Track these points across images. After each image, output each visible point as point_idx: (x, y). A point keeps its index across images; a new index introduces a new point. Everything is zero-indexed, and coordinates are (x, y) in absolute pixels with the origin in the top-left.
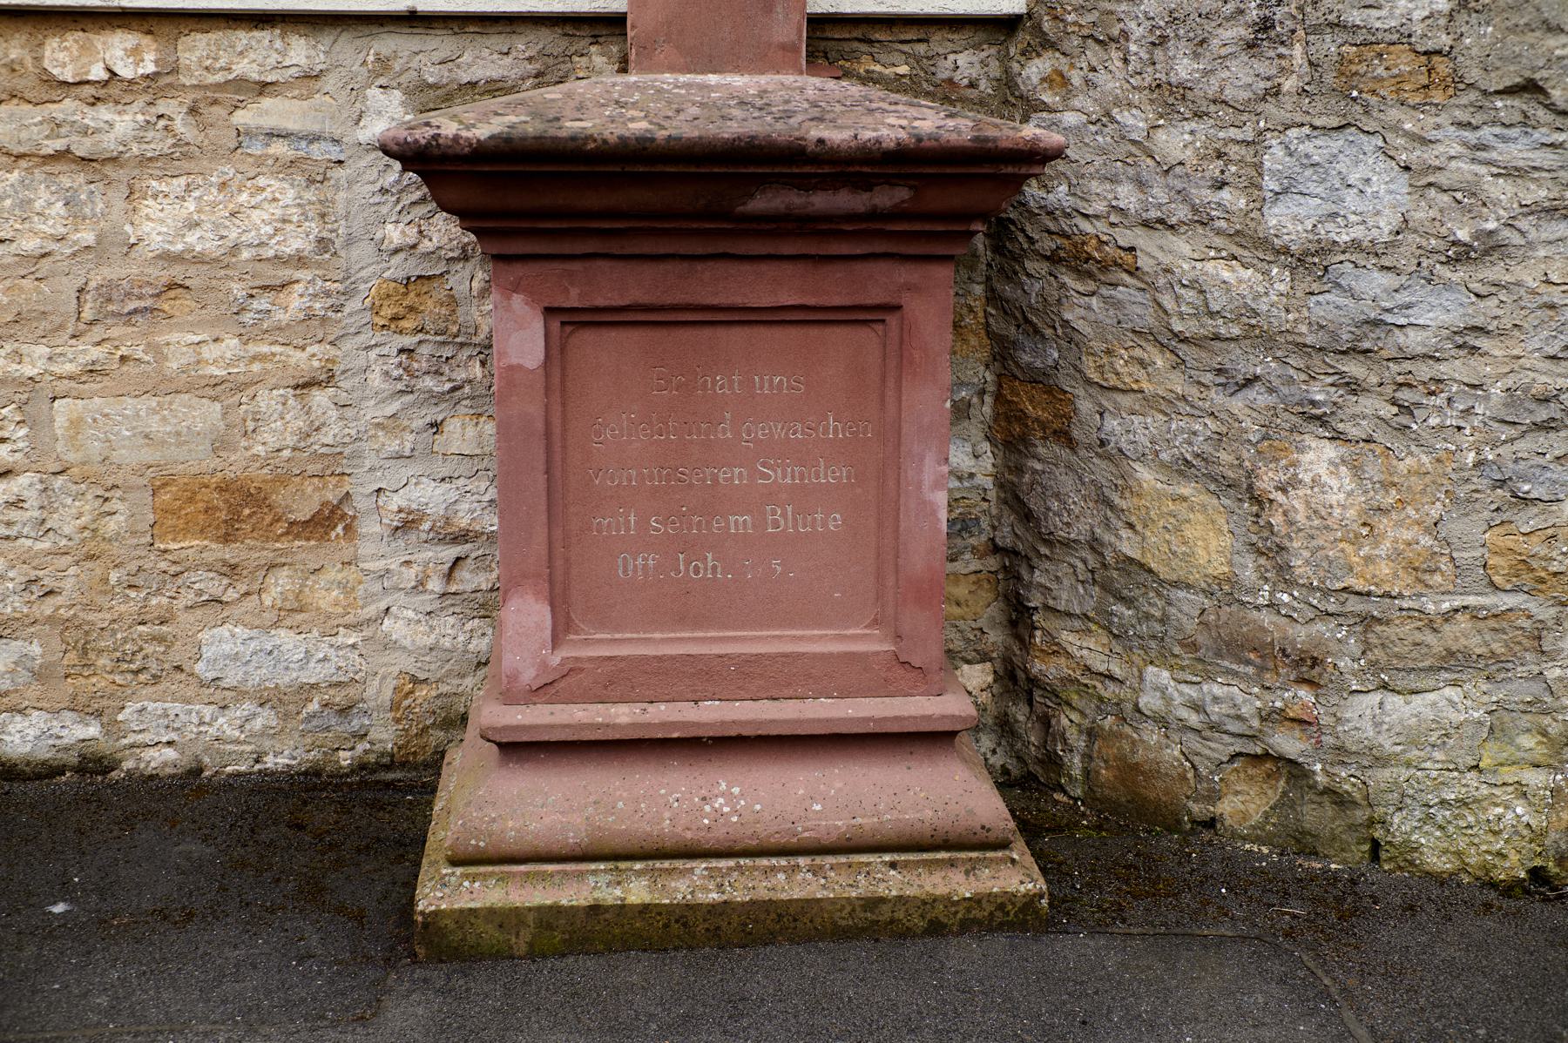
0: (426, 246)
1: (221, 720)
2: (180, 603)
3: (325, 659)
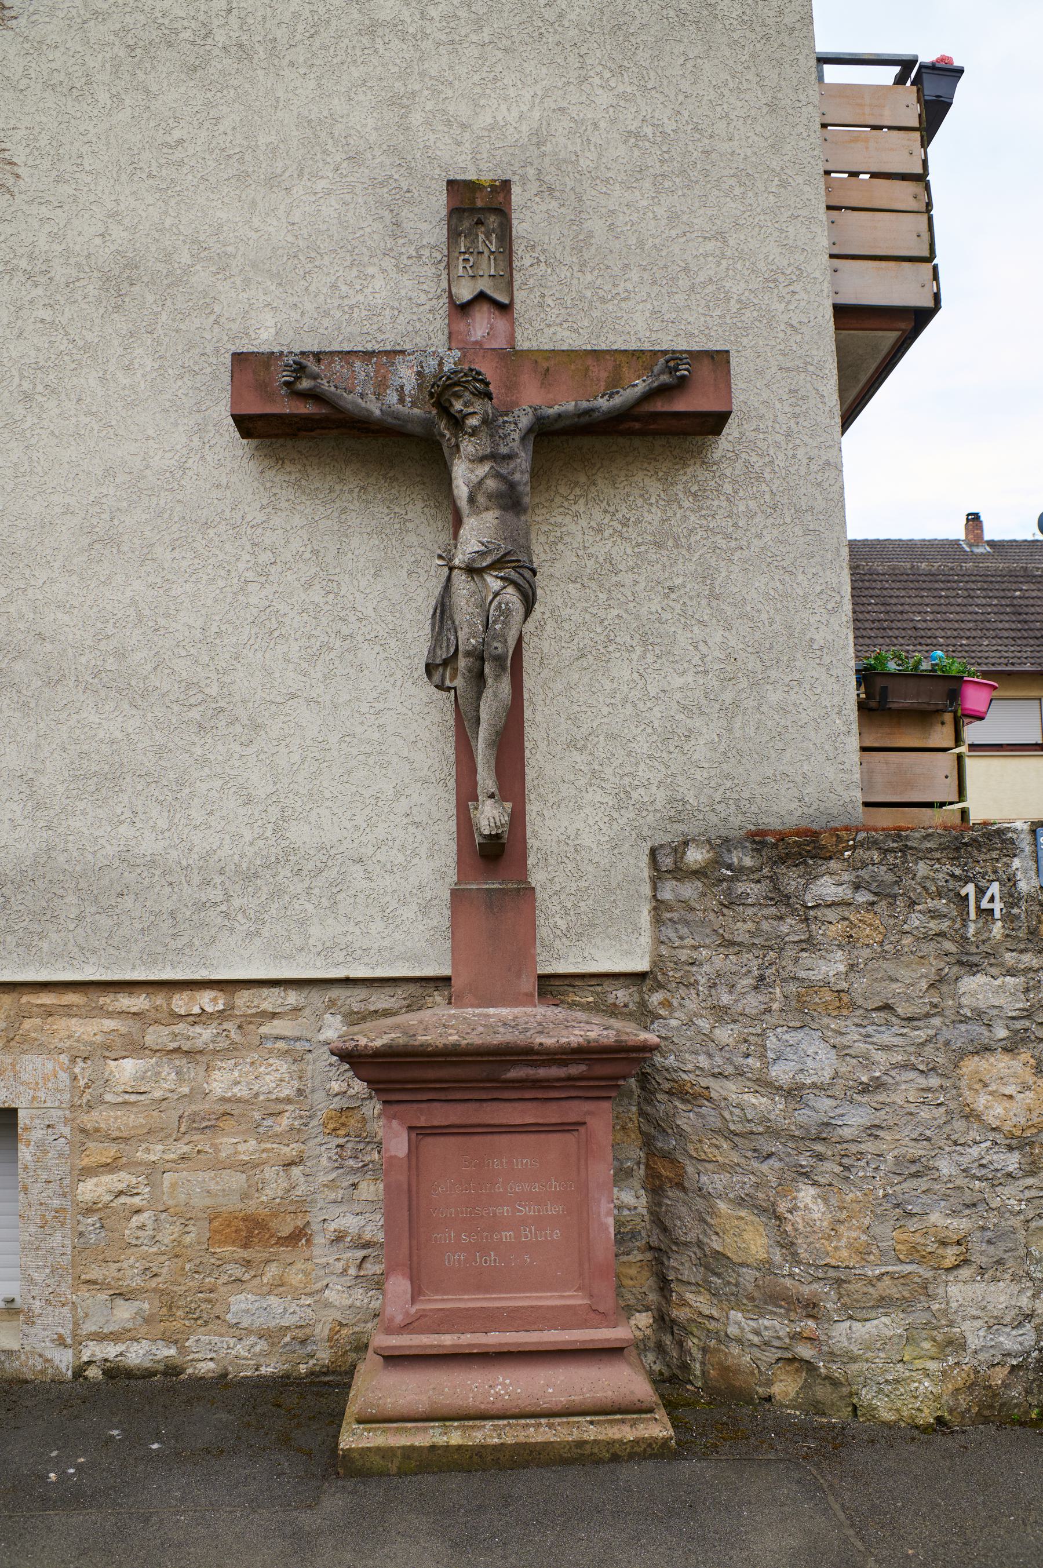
0: (352, 1092)
1: (239, 1346)
2: (220, 1281)
3: (294, 1313)
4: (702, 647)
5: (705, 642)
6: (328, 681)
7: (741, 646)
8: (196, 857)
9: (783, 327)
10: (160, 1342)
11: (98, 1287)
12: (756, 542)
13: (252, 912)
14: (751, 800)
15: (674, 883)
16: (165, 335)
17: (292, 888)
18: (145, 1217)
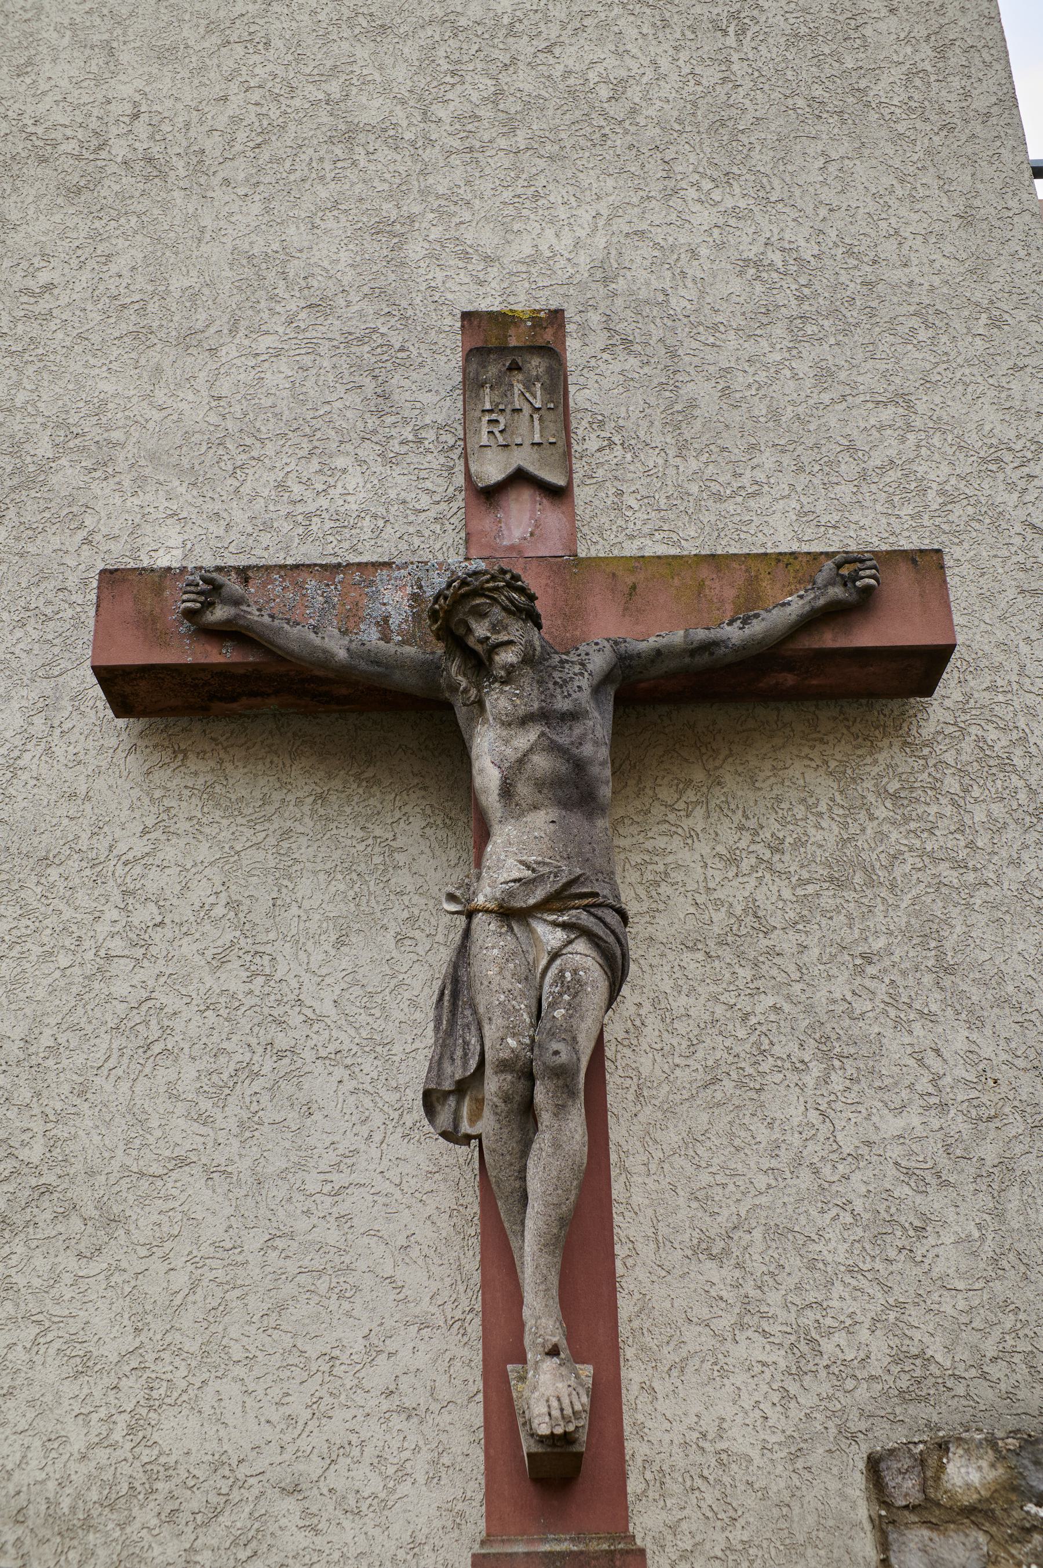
4: (931, 1059)
5: (937, 1051)
6: (248, 1134)
7: (1004, 1056)
9: (1018, 528)
12: (1010, 872)
15: (926, 1533)
17: (157, 1550)
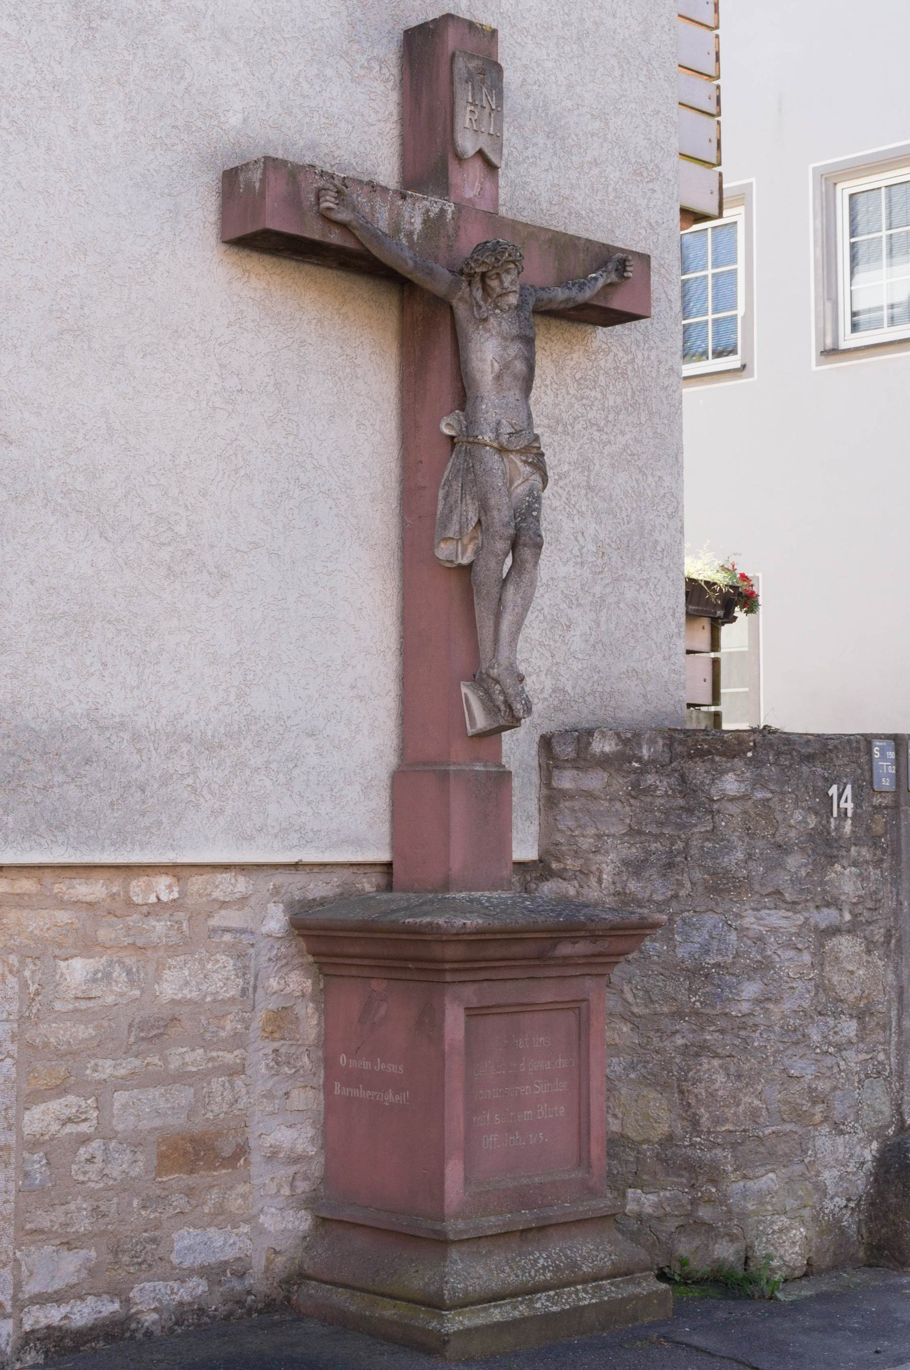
0: (288, 990)
1: (182, 1290)
2: (164, 1217)
3: (234, 1243)
4: (580, 538)
5: (583, 534)
6: (287, 533)
7: (608, 541)
8: (164, 721)
9: (644, 224)
10: (105, 1296)
11: (44, 1237)
12: (620, 438)
13: (217, 786)
14: (611, 695)
15: (575, 772)
16: (137, 93)
17: (253, 761)
18: (96, 1145)
